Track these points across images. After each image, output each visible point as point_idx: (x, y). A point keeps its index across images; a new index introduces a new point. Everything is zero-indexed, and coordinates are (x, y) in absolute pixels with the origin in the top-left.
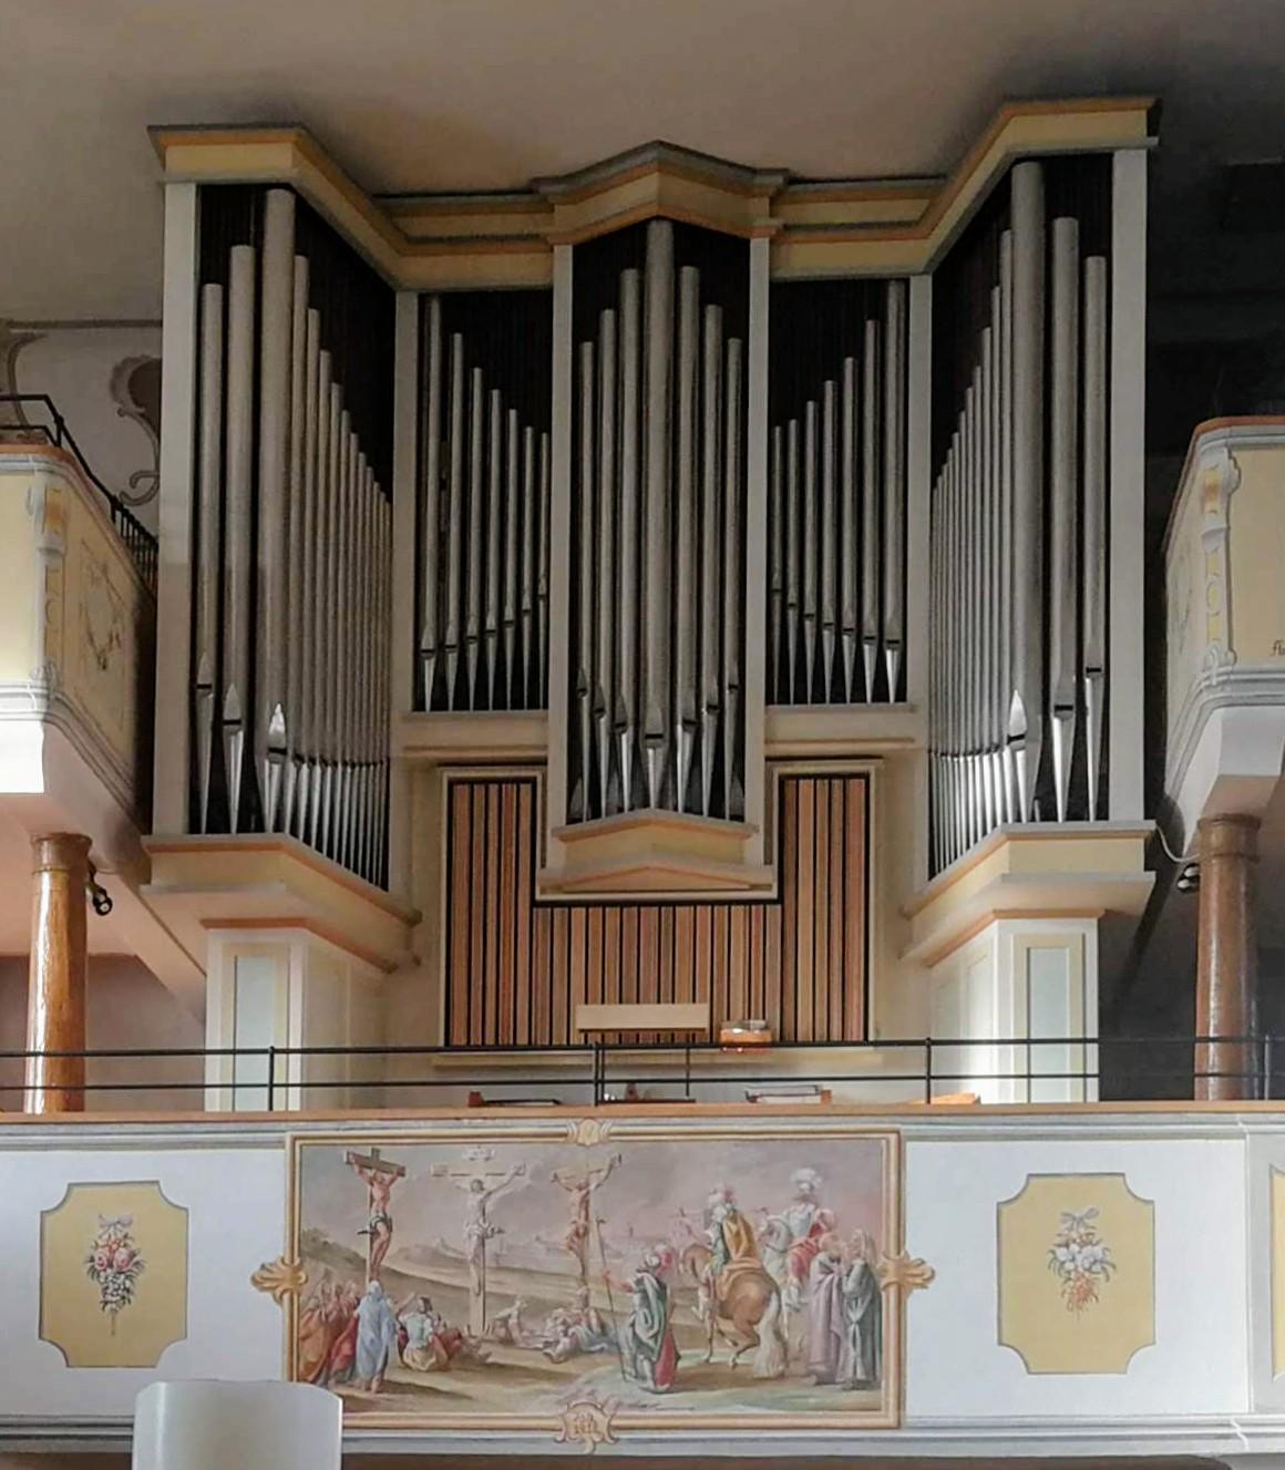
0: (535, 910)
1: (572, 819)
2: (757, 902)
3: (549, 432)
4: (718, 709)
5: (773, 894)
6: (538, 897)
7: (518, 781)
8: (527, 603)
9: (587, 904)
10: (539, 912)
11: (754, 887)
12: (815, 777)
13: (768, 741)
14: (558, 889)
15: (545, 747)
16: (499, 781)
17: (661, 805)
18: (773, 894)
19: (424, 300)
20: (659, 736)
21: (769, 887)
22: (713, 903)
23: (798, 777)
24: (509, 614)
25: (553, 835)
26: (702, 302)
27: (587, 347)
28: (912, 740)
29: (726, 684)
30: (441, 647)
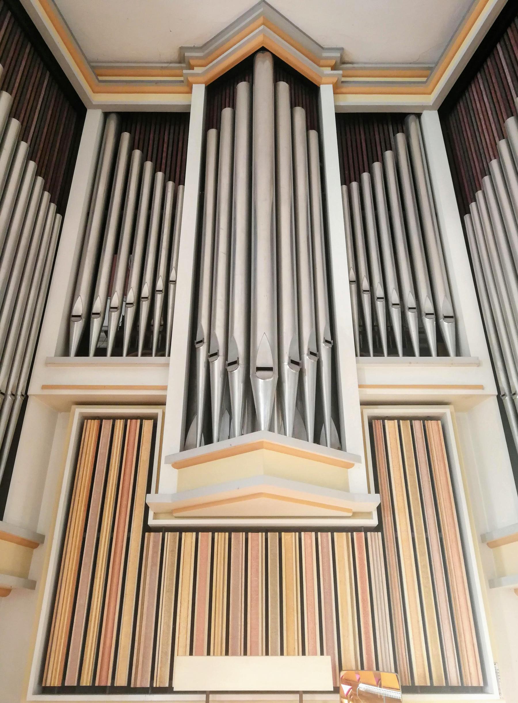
0: (147, 534)
1: (184, 446)
2: (358, 529)
3: (184, 185)
4: (315, 354)
5: (374, 522)
6: (151, 522)
7: (142, 418)
8: (160, 285)
9: (197, 530)
10: (153, 538)
11: (355, 515)
12: (399, 419)
13: (360, 386)
14: (171, 513)
15: (165, 388)
16: (126, 418)
17: (271, 429)
18: (374, 522)
19: (106, 115)
20: (270, 369)
21: (368, 515)
22: (317, 530)
23: (383, 419)
24: (146, 291)
25: (166, 463)
26: (293, 105)
27: (213, 133)
28: (481, 387)
29: (322, 340)
30: (89, 313)
